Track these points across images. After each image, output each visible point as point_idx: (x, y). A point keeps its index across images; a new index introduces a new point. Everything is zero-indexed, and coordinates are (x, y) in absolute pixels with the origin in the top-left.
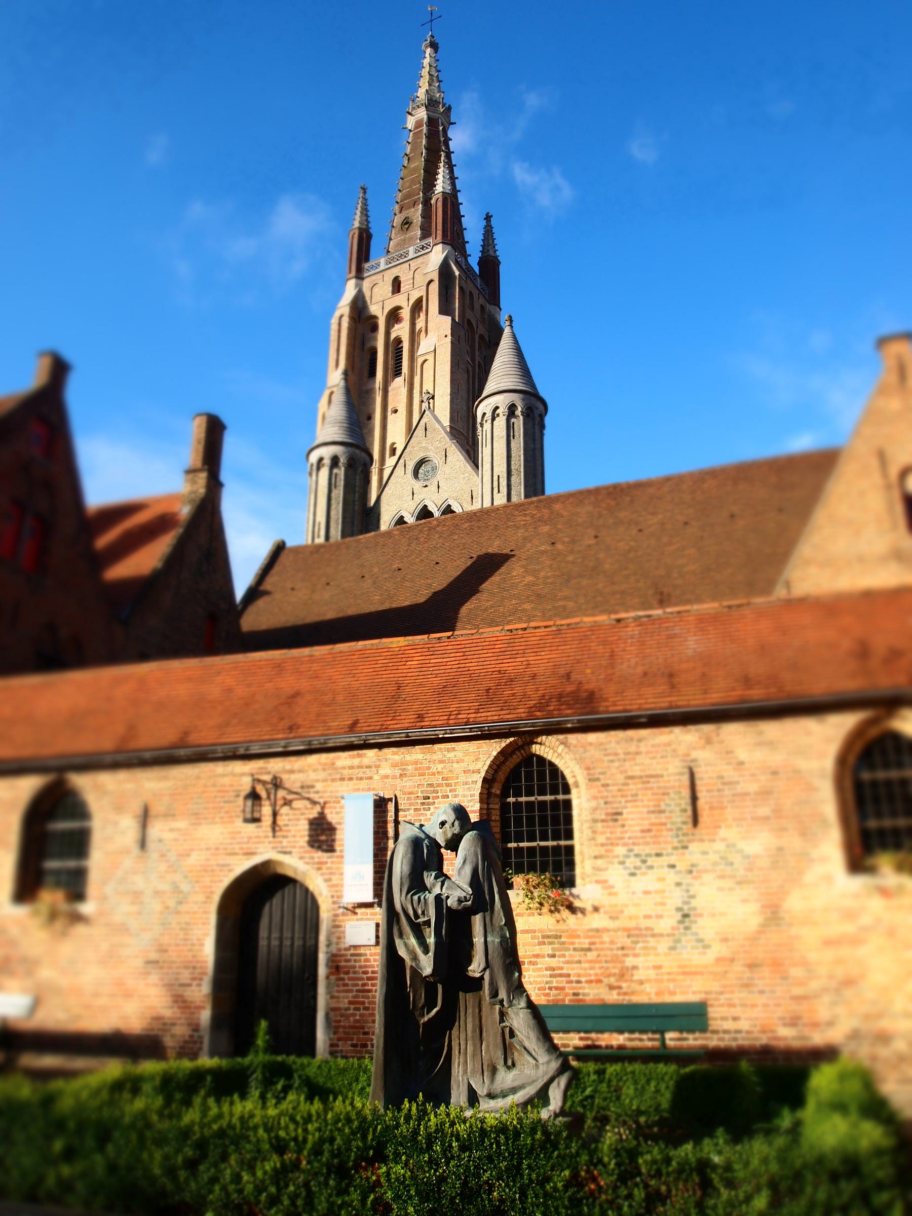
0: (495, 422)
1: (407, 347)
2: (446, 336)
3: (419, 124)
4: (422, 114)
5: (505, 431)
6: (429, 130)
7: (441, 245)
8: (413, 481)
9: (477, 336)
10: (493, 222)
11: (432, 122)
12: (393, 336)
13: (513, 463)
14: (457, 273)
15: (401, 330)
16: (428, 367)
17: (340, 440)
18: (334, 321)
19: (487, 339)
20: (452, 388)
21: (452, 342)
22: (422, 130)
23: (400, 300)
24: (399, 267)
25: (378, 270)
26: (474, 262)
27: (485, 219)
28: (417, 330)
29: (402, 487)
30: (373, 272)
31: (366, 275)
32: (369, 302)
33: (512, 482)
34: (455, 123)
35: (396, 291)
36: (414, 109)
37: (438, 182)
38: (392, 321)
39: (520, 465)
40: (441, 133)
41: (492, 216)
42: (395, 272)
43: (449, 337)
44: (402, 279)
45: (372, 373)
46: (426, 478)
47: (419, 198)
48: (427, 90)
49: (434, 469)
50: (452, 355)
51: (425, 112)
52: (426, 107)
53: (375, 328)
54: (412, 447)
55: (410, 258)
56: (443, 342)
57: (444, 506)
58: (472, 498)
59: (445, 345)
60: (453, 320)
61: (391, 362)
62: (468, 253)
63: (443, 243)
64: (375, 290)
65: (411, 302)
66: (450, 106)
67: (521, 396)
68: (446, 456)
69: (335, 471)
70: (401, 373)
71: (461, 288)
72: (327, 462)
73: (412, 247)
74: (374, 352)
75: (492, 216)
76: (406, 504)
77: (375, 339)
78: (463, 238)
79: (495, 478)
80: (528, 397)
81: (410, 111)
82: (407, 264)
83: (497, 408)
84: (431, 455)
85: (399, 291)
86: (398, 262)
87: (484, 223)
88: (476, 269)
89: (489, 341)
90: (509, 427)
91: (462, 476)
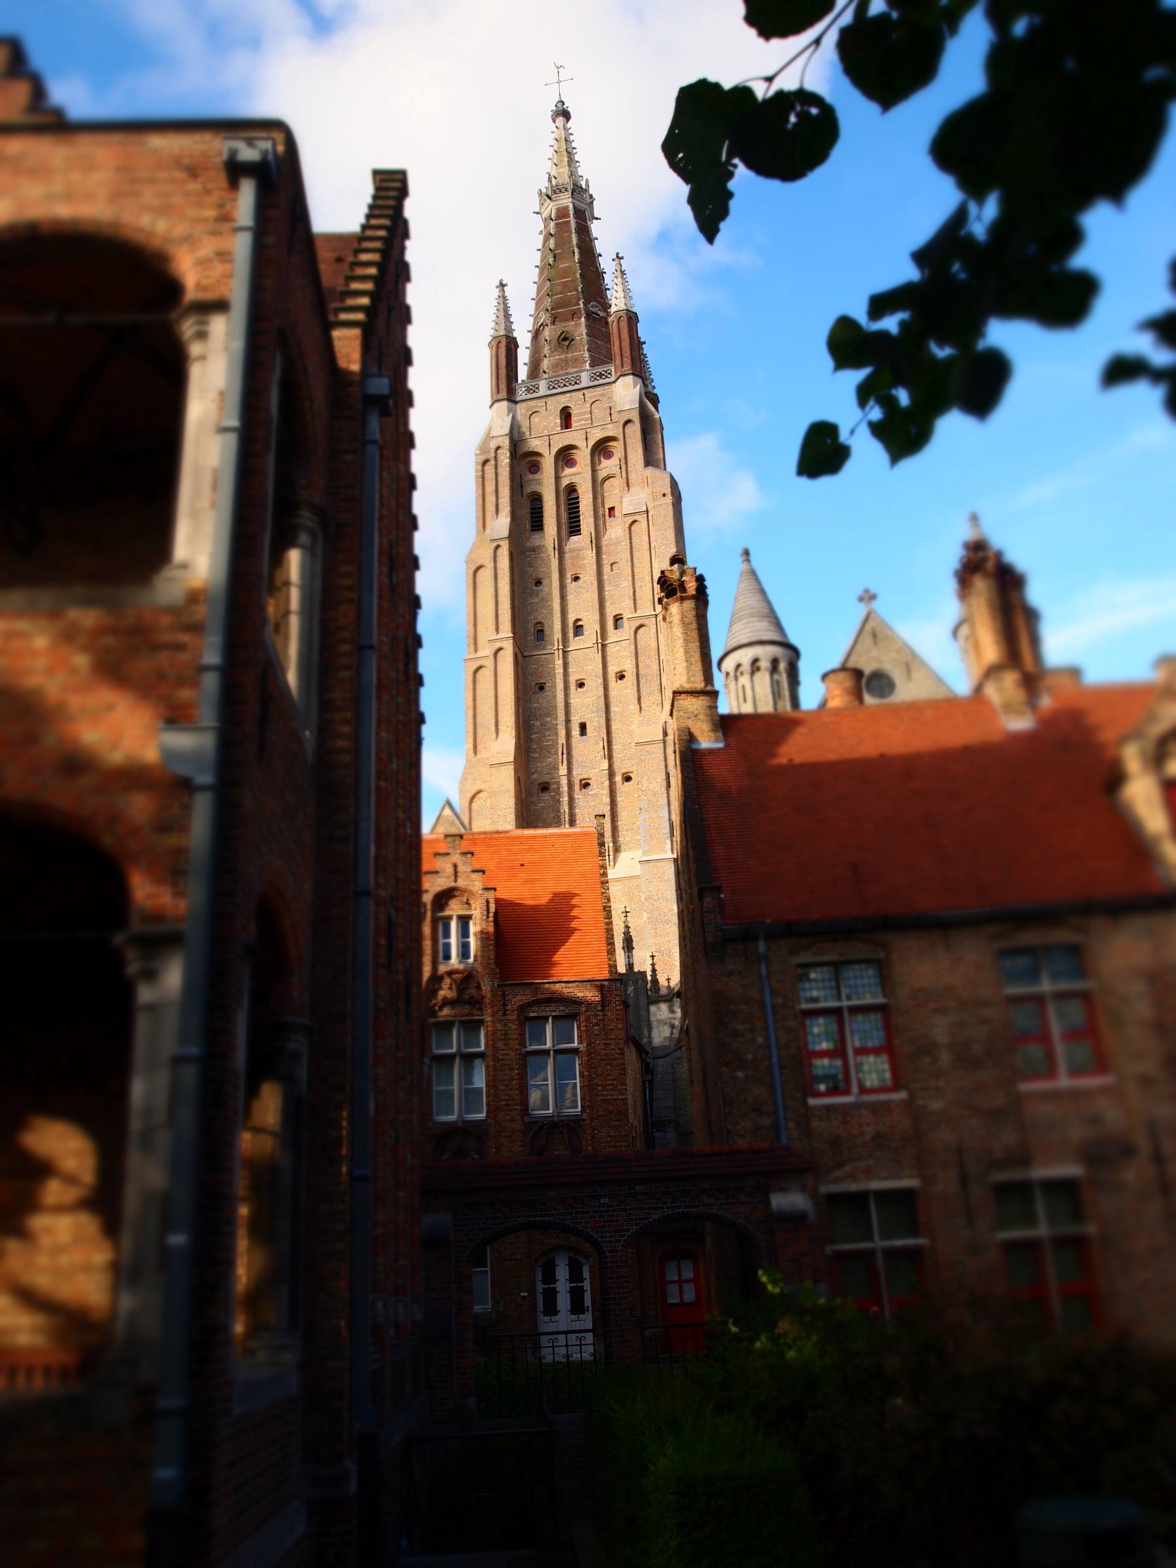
2: (664, 495)
12: (565, 482)
15: (579, 474)
24: (568, 395)
25: (535, 395)
32: (527, 433)
34: (600, 219)
42: (564, 401)
56: (661, 502)
72: (765, 664)
77: (539, 482)
82: (581, 393)
86: (565, 389)
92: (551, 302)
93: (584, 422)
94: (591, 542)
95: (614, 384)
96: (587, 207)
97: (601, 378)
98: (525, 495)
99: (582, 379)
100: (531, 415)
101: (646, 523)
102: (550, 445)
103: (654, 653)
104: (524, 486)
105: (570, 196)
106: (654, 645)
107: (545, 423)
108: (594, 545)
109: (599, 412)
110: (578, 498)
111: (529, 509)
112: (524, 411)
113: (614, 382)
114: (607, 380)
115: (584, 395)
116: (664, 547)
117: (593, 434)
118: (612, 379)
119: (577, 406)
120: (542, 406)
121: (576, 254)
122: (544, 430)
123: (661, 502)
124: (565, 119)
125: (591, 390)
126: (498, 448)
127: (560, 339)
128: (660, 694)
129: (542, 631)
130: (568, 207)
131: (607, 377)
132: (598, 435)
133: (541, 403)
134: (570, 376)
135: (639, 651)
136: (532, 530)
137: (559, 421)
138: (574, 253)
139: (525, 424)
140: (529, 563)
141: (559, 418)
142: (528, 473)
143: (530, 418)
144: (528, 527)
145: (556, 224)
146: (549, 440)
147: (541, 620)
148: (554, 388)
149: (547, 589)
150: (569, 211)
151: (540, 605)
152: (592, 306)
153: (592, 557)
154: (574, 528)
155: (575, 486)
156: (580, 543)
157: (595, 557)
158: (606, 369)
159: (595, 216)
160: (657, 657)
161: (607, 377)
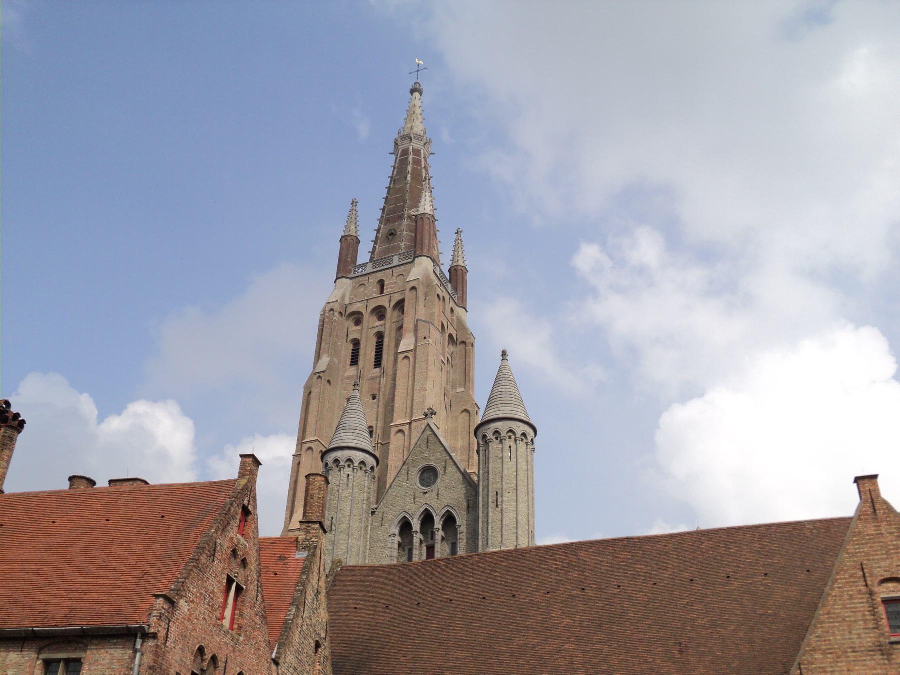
2: (425, 338)
9: (447, 335)
10: (463, 236)
23: (384, 302)
26: (446, 270)
42: (380, 276)
70: (380, 364)
75: (461, 232)
82: (391, 270)
86: (383, 268)
89: (457, 340)
96: (423, 148)
98: (349, 340)
102: (367, 306)
111: (351, 350)
113: (413, 262)
115: (393, 272)
117: (395, 297)
119: (388, 279)
132: (398, 298)
134: (386, 260)
144: (349, 362)
152: (413, 212)
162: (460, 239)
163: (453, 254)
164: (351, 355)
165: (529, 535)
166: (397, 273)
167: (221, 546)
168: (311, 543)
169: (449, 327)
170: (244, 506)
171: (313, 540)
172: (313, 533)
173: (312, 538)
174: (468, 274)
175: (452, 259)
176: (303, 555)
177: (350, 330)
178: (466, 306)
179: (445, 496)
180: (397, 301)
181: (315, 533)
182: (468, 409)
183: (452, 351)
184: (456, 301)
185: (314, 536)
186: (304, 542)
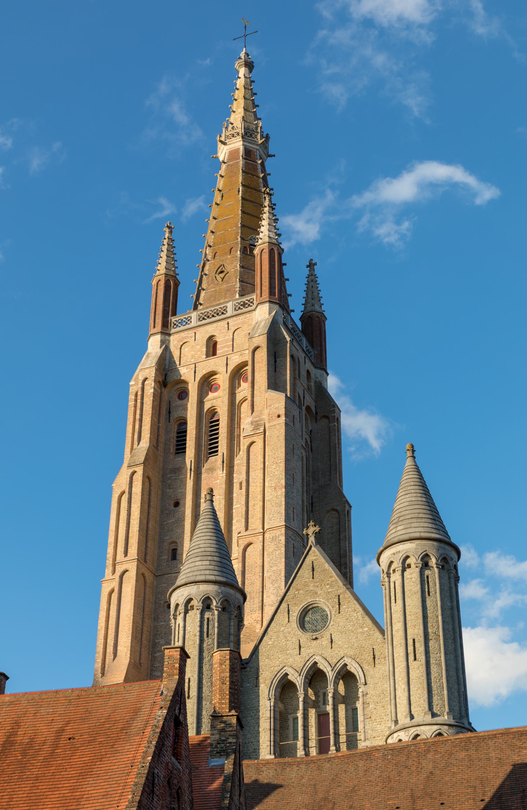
0: (406, 574)
1: (226, 422)
3: (233, 154)
4: (238, 144)
5: (419, 587)
6: (246, 165)
7: (267, 305)
8: (299, 632)
9: (304, 408)
11: (248, 153)
13: (429, 625)
14: (288, 339)
16: (257, 450)
17: (212, 578)
18: (134, 386)
19: (314, 411)
20: (287, 479)
21: (286, 424)
22: (238, 163)
24: (215, 325)
26: (296, 316)
27: (308, 267)
28: (237, 402)
29: (286, 637)
30: (182, 328)
31: (173, 331)
32: (177, 363)
33: (431, 648)
34: (274, 156)
35: (211, 352)
36: (227, 137)
37: (262, 229)
38: (206, 388)
39: (438, 627)
40: (259, 167)
41: (315, 264)
43: (283, 418)
44: (219, 339)
45: (181, 448)
46: (314, 628)
47: (237, 243)
48: (243, 117)
49: (325, 619)
50: (286, 440)
51: (241, 143)
52: (243, 137)
53: (183, 394)
54: (298, 590)
55: (229, 314)
56: (274, 423)
57: (339, 666)
58: (374, 658)
59: (277, 427)
60: (286, 395)
61: (205, 439)
62: (291, 308)
63: (270, 302)
64: (185, 349)
65: (231, 368)
66: (267, 135)
67: (435, 543)
68: (339, 604)
69: (207, 615)
70: (217, 451)
71: (292, 356)
72: (196, 603)
73: (231, 303)
74: (183, 423)
76: (291, 660)
77: (186, 409)
78: (286, 292)
79: (410, 642)
80: (443, 545)
81: (223, 139)
82: (225, 322)
83: (407, 557)
84: (323, 602)
85: (214, 353)
87: (307, 271)
88: (299, 324)
89: (316, 413)
90: (424, 581)
91: (361, 630)
92: (214, 239)
93: (226, 349)
94: (223, 462)
95: (254, 312)
97: (244, 307)
99: (228, 310)
100: (182, 346)
101: (262, 444)
102: (195, 372)
103: (259, 570)
104: (171, 411)
105: (241, 139)
106: (260, 562)
107: (193, 353)
108: (225, 465)
109: (241, 338)
110: (218, 420)
111: (175, 433)
112: (176, 342)
113: (254, 310)
114: (250, 308)
115: (228, 324)
116: (274, 467)
118: (254, 306)
120: (191, 337)
121: (240, 193)
122: (192, 358)
123: (274, 423)
124: (247, 69)
125: (235, 318)
126: (146, 379)
127: (218, 272)
128: (260, 612)
129: (176, 549)
130: (239, 149)
131: (249, 305)
133: (191, 333)
135: (246, 568)
136: (176, 453)
137: (205, 349)
138: (239, 191)
139: (176, 354)
140: (169, 485)
141: (205, 346)
142: (177, 399)
143: (181, 349)
145: (228, 166)
146: (195, 367)
147: (175, 540)
148: (204, 319)
149: (183, 509)
150: (239, 153)
151: (176, 524)
153: (223, 476)
154: (213, 450)
155: (216, 409)
156: (216, 461)
157: (225, 477)
158: (248, 298)
159: (270, 153)
160: (261, 574)
161: (249, 305)
162: (313, 274)
163: (305, 296)
164: (175, 439)
165: (459, 698)
166: (234, 326)
167: (158, 776)
168: (228, 745)
169: (306, 396)
170: (176, 715)
171: (230, 740)
172: (229, 731)
173: (228, 738)
174: (327, 322)
175: (304, 303)
176: (217, 761)
177: (173, 405)
178: (326, 366)
179: (340, 643)
180: (237, 364)
181: (232, 731)
182: (335, 507)
183: (310, 428)
184: (313, 361)
185: (230, 735)
186: (219, 744)
